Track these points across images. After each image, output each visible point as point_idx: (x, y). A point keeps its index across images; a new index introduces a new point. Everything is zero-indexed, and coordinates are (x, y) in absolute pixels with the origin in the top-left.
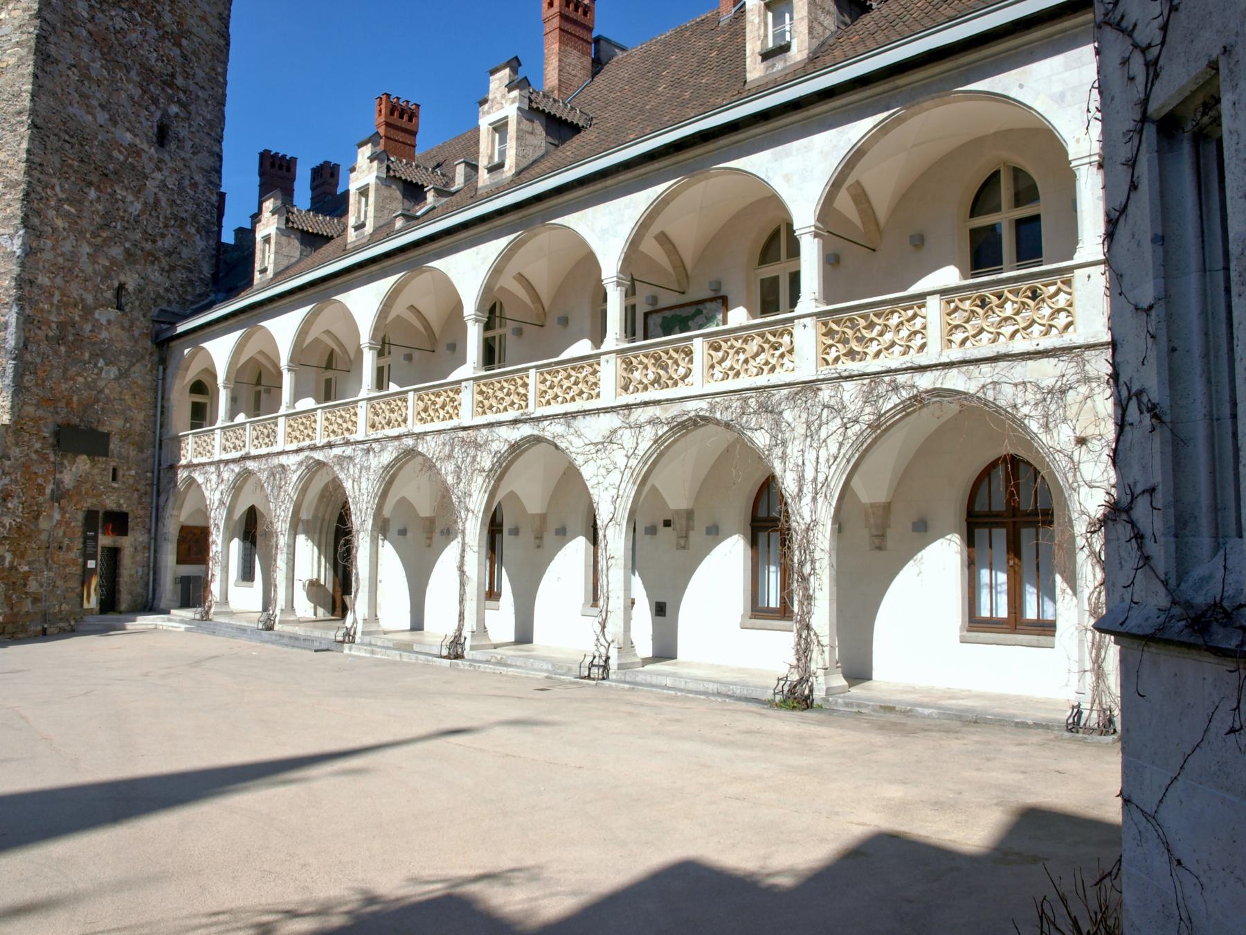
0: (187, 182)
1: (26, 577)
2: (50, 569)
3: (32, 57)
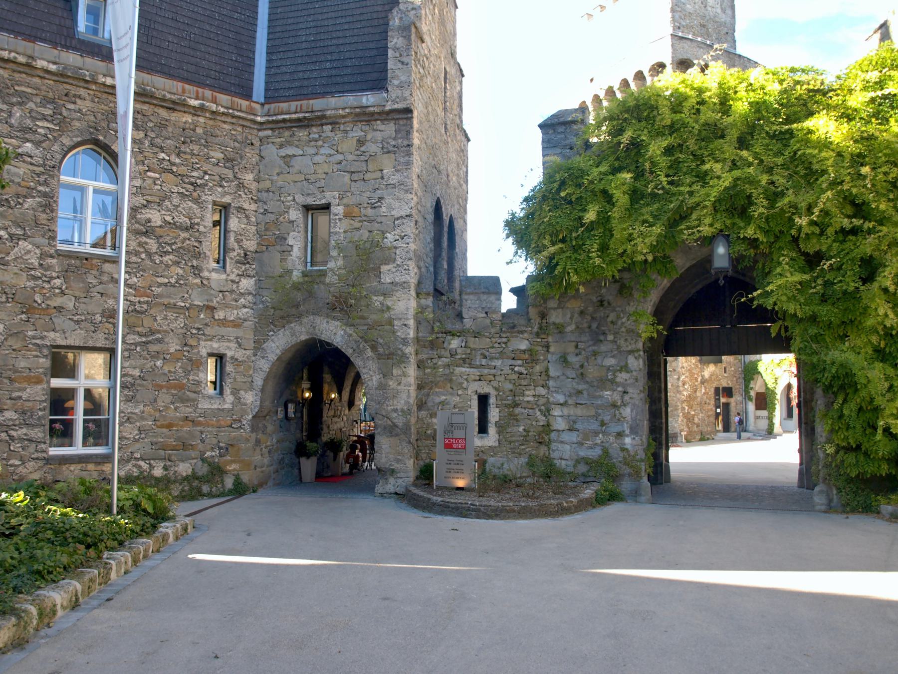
1: (694, 415)
2: (702, 413)
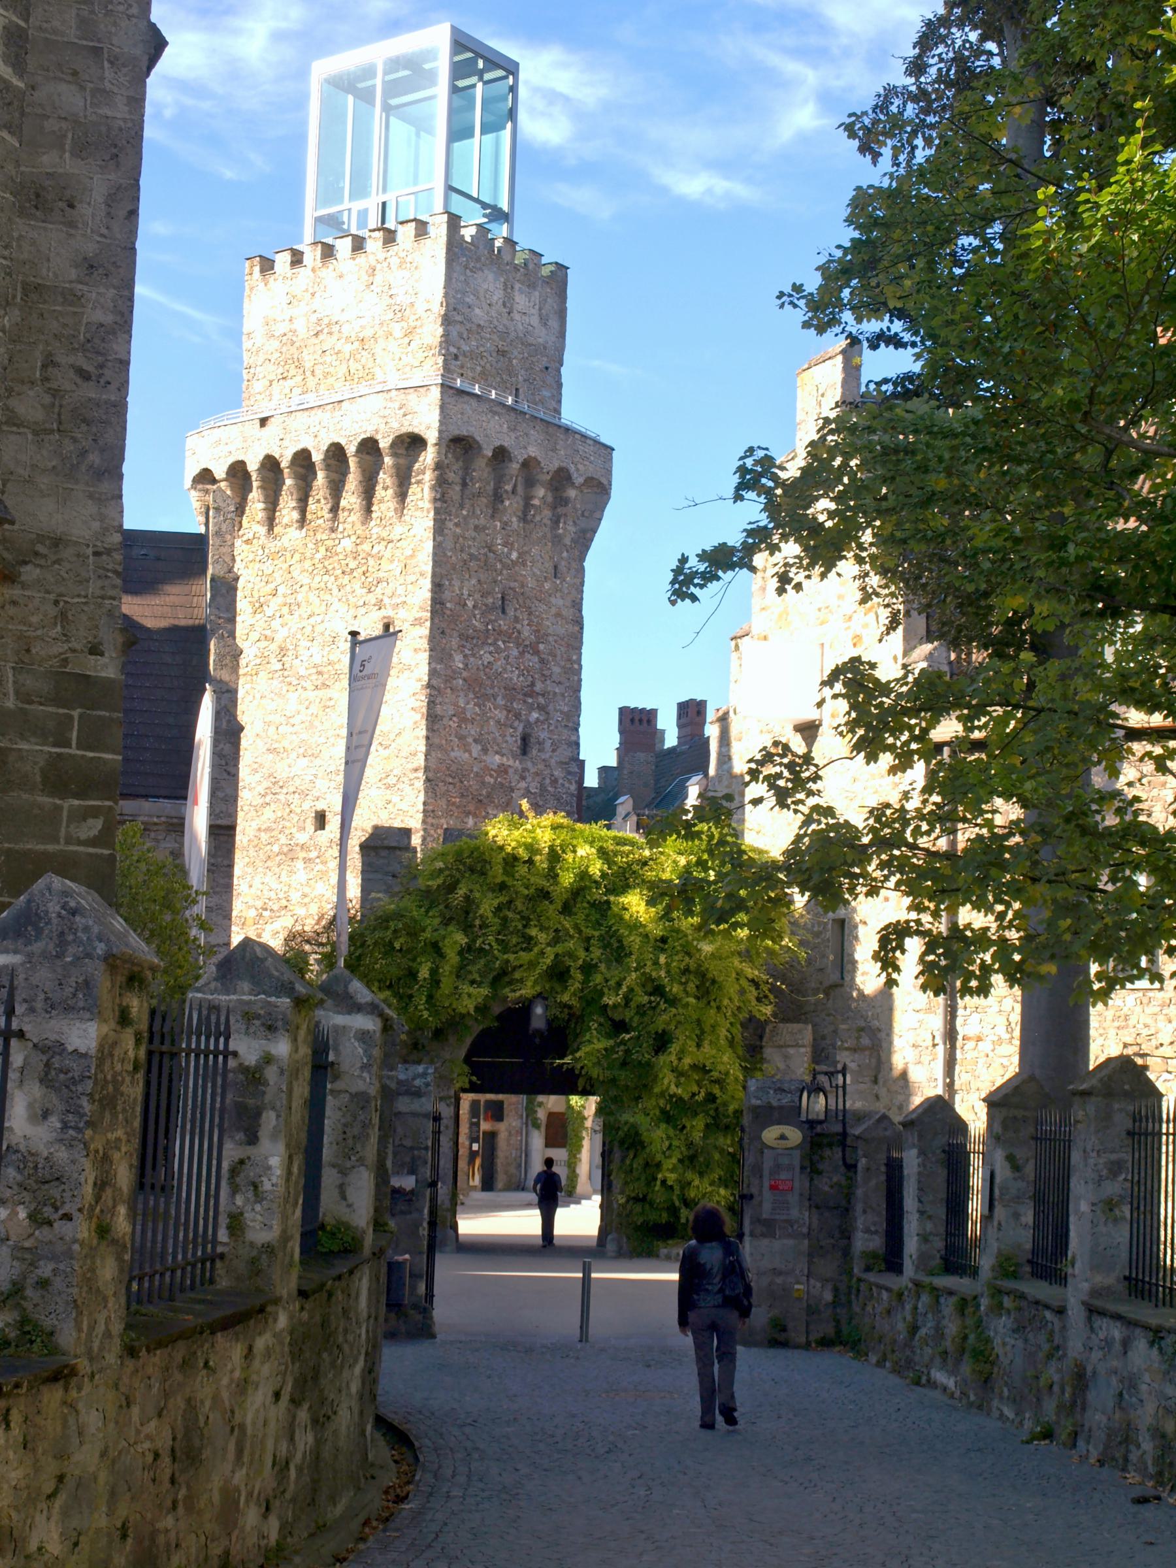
0: (548, 781)
3: (424, 722)
